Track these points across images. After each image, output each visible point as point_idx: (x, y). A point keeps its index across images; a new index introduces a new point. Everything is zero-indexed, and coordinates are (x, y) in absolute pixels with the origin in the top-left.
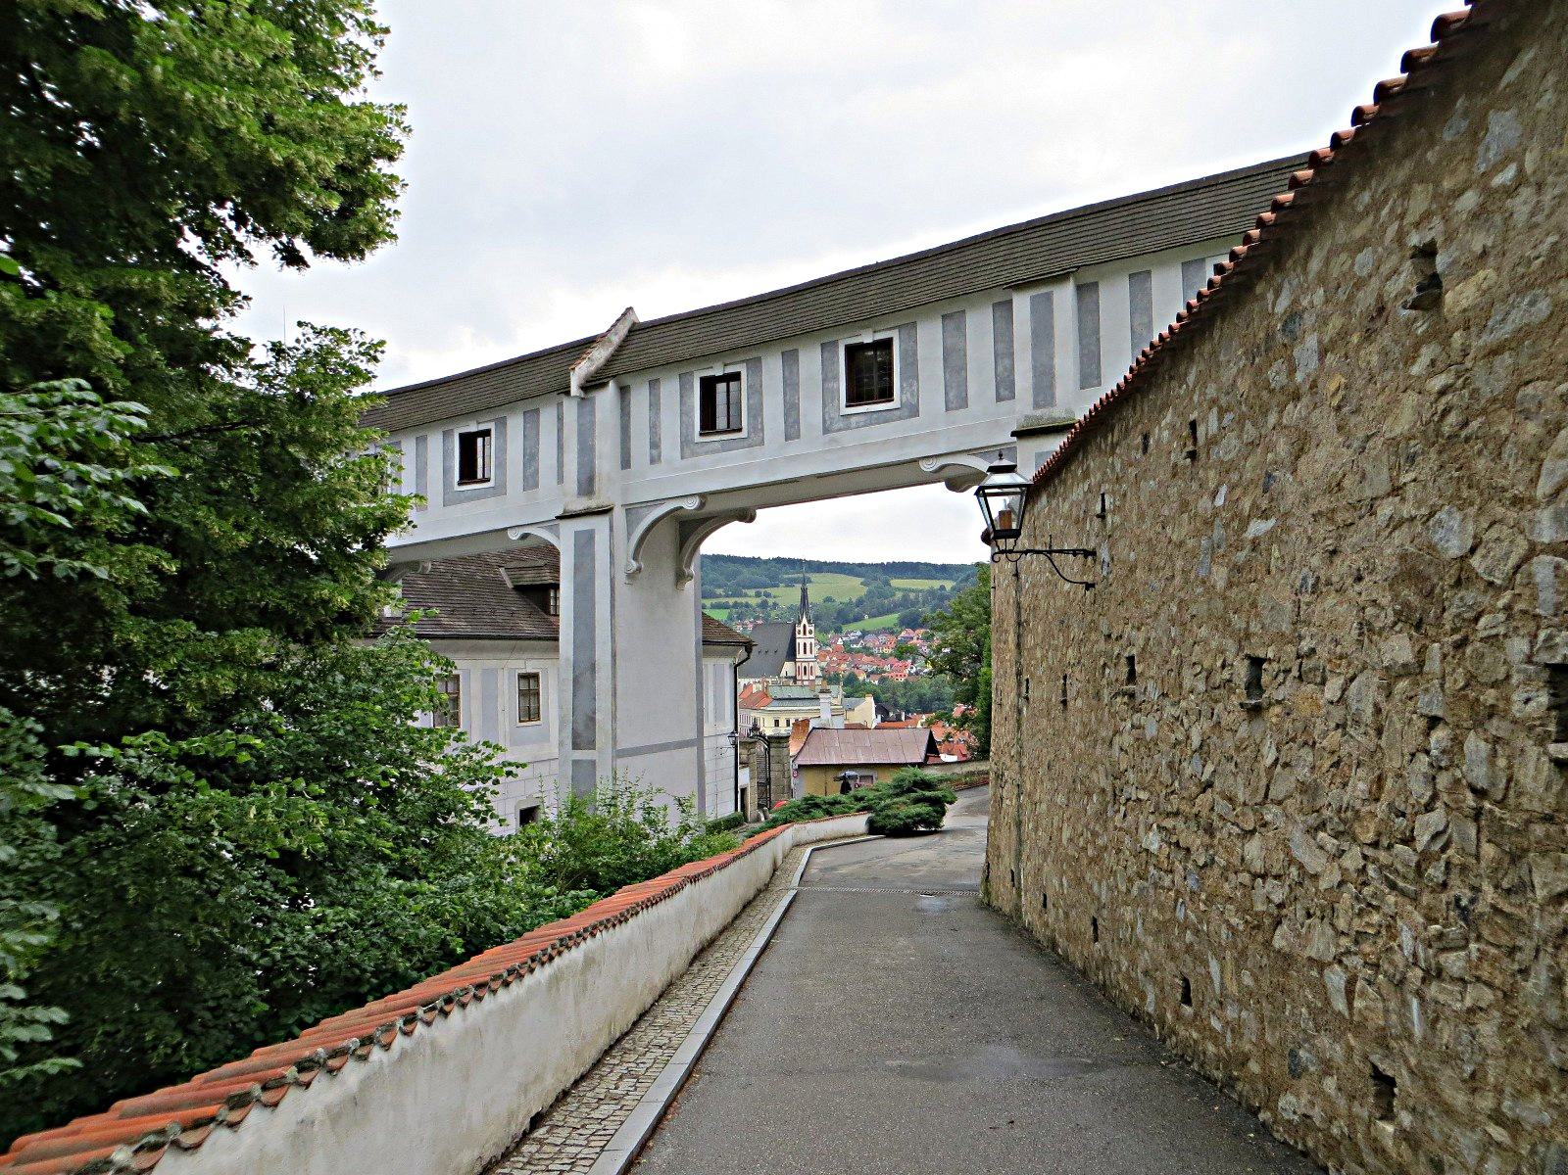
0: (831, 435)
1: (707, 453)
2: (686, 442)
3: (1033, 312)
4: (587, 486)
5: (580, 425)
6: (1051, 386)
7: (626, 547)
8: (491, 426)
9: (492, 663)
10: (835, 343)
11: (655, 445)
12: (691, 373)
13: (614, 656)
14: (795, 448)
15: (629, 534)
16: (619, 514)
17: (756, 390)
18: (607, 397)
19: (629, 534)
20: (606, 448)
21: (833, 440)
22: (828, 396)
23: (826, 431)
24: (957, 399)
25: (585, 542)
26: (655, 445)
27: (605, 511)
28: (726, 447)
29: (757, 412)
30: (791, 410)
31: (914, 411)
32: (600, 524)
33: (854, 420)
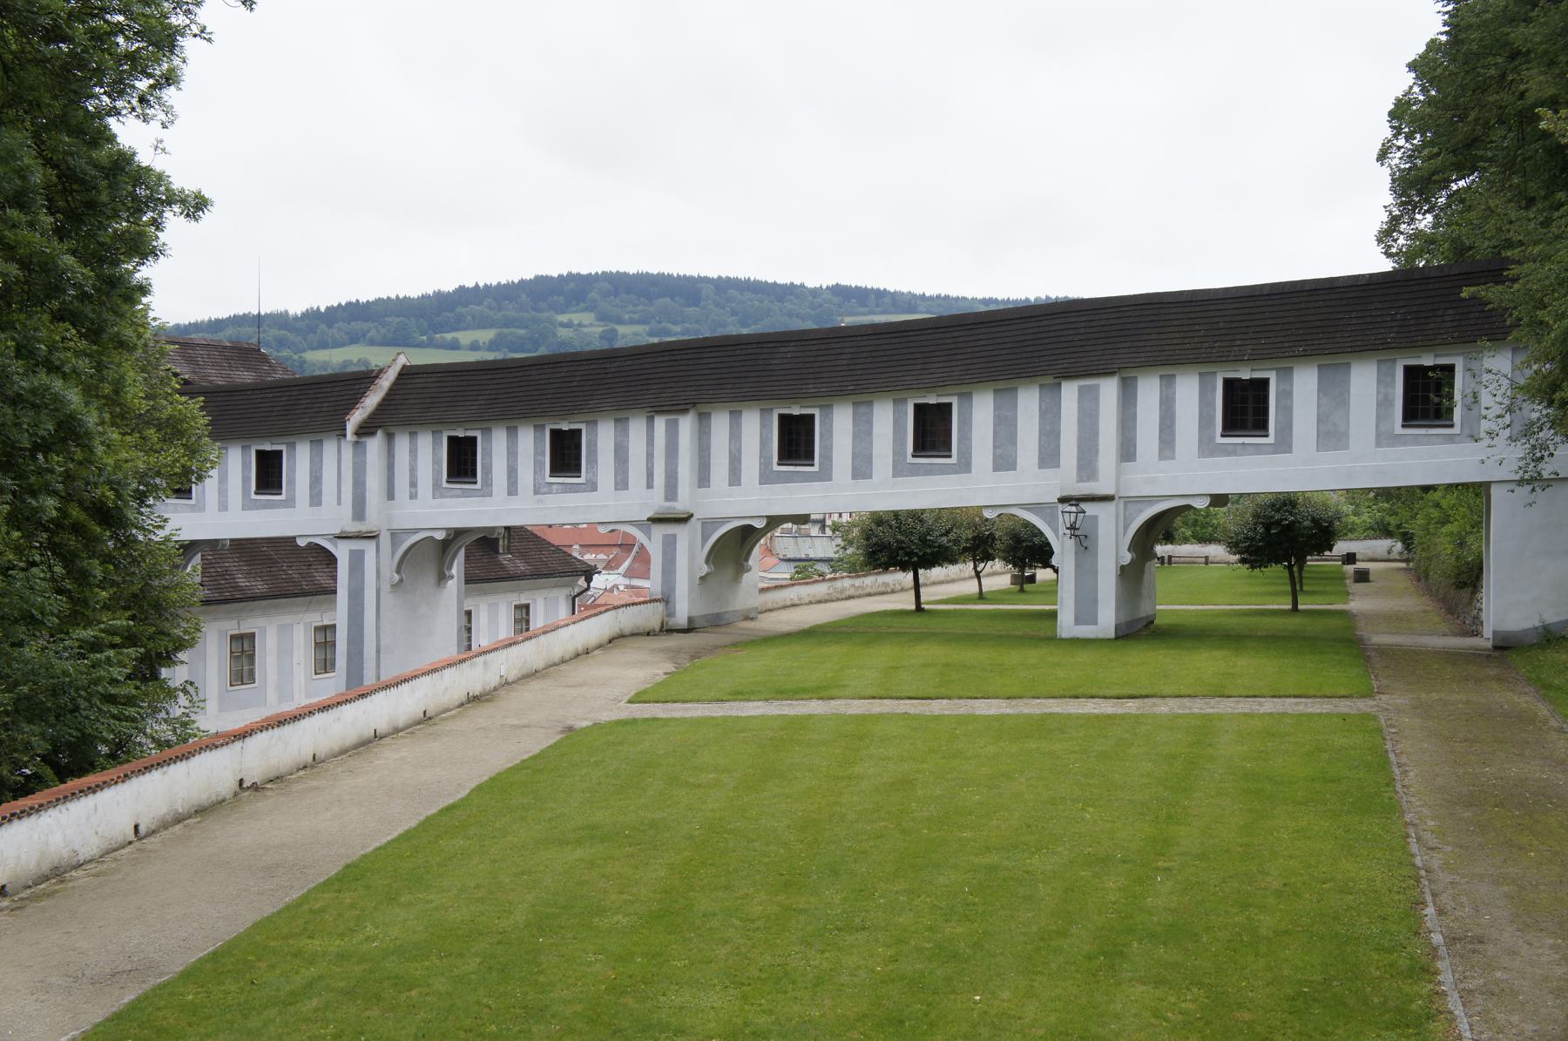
0: (539, 496)
1: (452, 497)
2: (436, 485)
3: (667, 431)
4: (359, 512)
5: (354, 463)
6: (675, 486)
7: (389, 563)
8: (283, 448)
9: (287, 619)
10: (543, 427)
11: (413, 484)
12: (441, 432)
13: (378, 652)
14: (514, 503)
15: (393, 553)
16: (385, 540)
17: (488, 454)
18: (375, 444)
19: (393, 553)
20: (374, 483)
21: (539, 501)
22: (538, 466)
23: (536, 492)
24: (622, 483)
25: (357, 560)
26: (413, 484)
27: (371, 536)
28: (465, 494)
29: (488, 470)
30: (512, 473)
31: (592, 486)
32: (369, 548)
33: (554, 487)
